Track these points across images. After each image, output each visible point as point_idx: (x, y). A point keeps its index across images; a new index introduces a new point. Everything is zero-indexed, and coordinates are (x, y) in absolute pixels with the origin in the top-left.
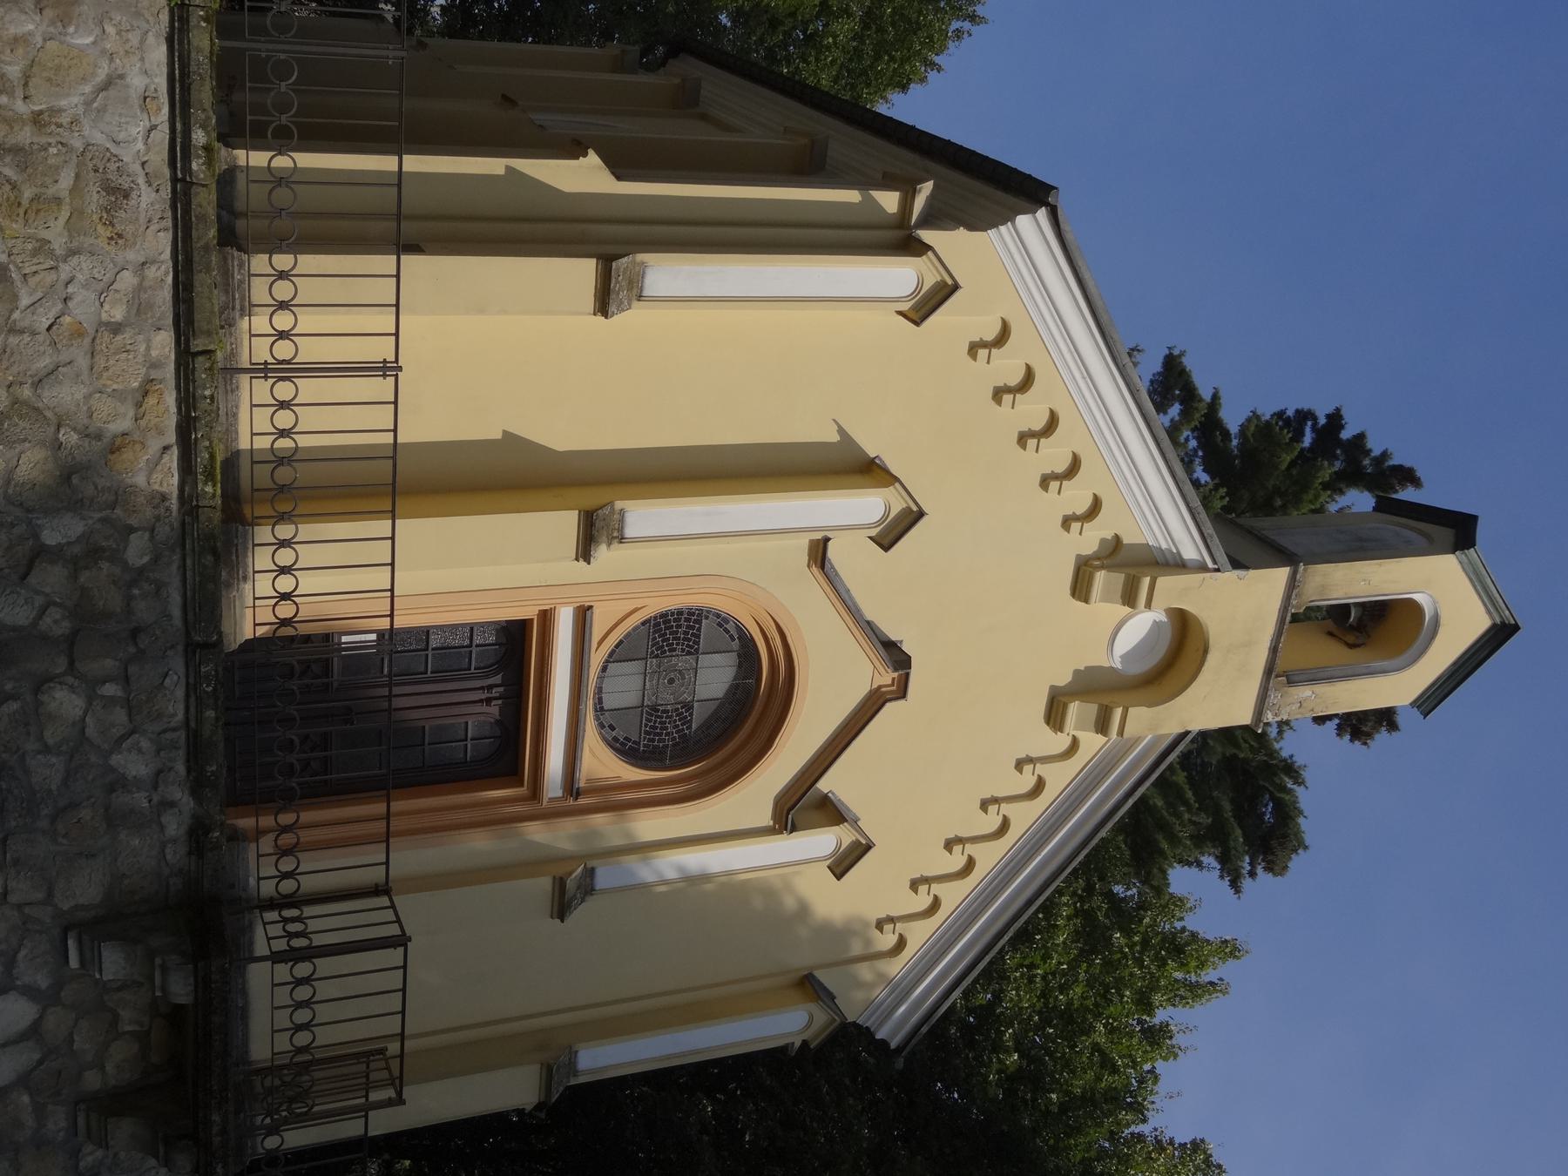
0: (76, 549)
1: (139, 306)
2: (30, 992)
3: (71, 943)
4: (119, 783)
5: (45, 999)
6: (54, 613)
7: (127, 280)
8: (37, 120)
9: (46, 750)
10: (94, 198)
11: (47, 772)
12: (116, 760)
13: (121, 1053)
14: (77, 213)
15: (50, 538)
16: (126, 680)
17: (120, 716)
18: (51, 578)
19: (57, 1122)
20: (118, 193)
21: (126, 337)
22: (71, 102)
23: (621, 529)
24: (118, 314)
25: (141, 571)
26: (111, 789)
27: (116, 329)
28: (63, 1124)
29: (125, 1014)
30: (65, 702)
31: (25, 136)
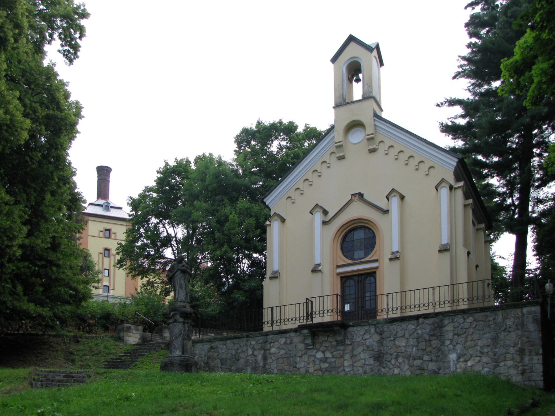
0: (253, 350)
1: (225, 344)
2: (316, 353)
3: (308, 347)
4: (285, 343)
5: (318, 350)
6: (261, 352)
7: (221, 346)
8: (205, 356)
9: (279, 352)
10: (212, 350)
11: (283, 352)
12: (282, 343)
13: (330, 339)
14: (214, 352)
15: (251, 353)
16: (271, 343)
17: (276, 343)
18: (256, 353)
19: (341, 348)
20: (212, 348)
21: (228, 346)
22: (203, 353)
23: (318, 264)
24: (225, 347)
25: (256, 342)
26: (287, 344)
27: (227, 347)
28: (341, 347)
29: (323, 339)
30: (273, 350)
31: (206, 357)
